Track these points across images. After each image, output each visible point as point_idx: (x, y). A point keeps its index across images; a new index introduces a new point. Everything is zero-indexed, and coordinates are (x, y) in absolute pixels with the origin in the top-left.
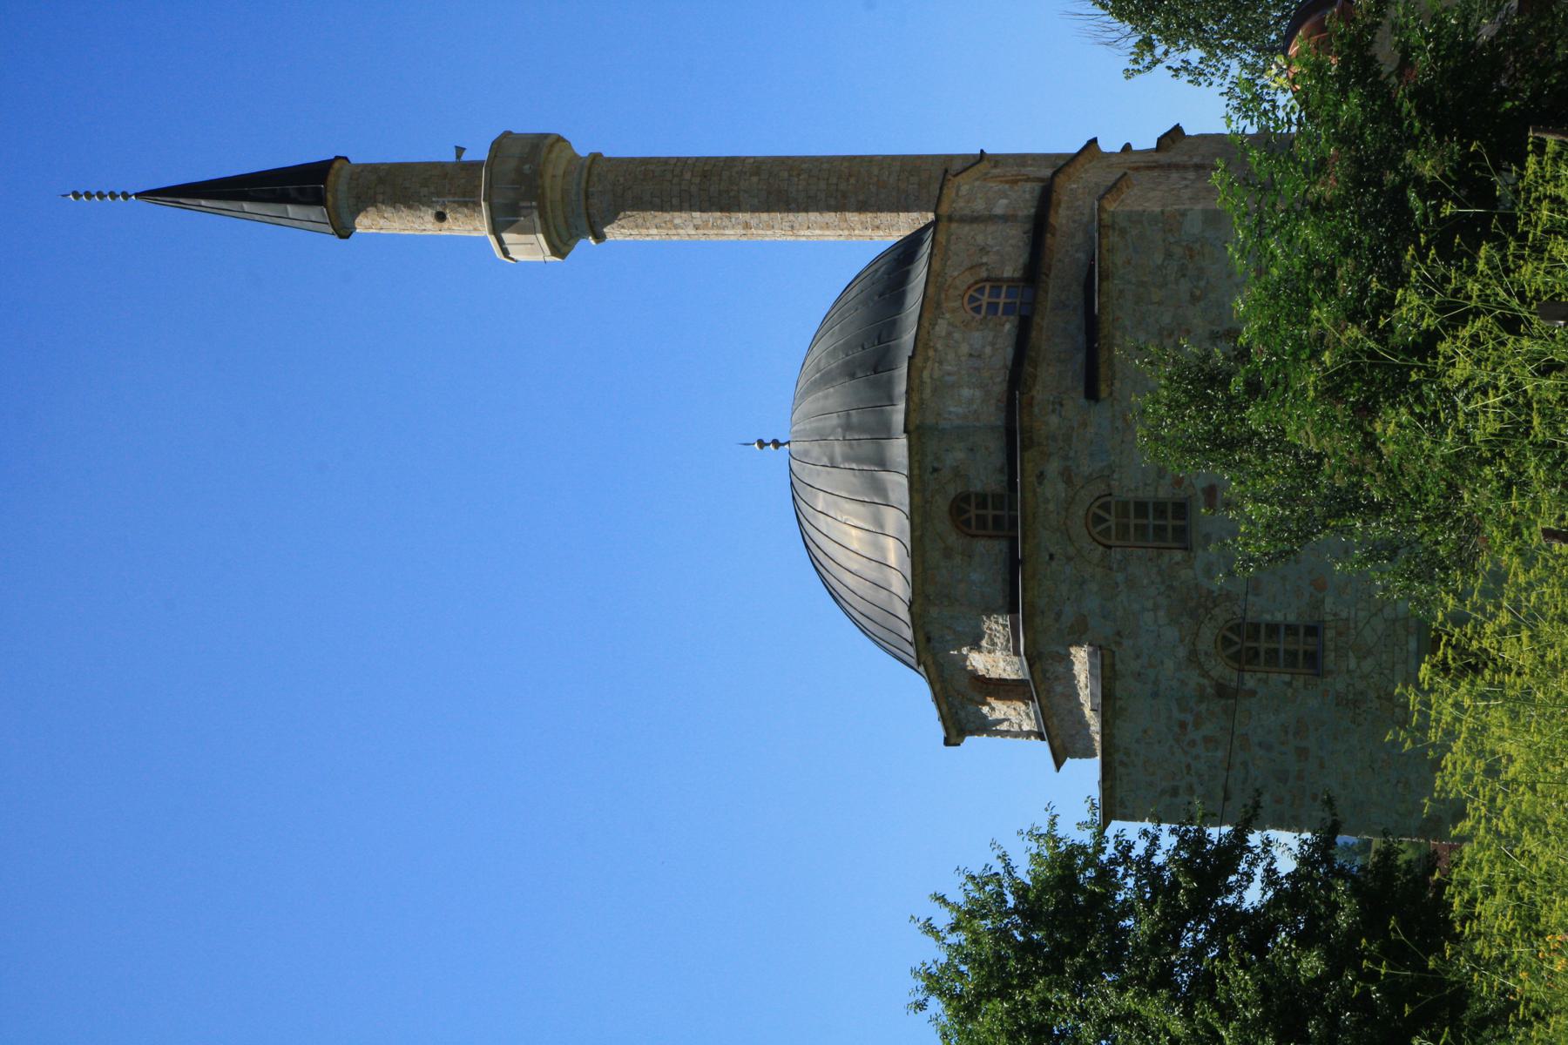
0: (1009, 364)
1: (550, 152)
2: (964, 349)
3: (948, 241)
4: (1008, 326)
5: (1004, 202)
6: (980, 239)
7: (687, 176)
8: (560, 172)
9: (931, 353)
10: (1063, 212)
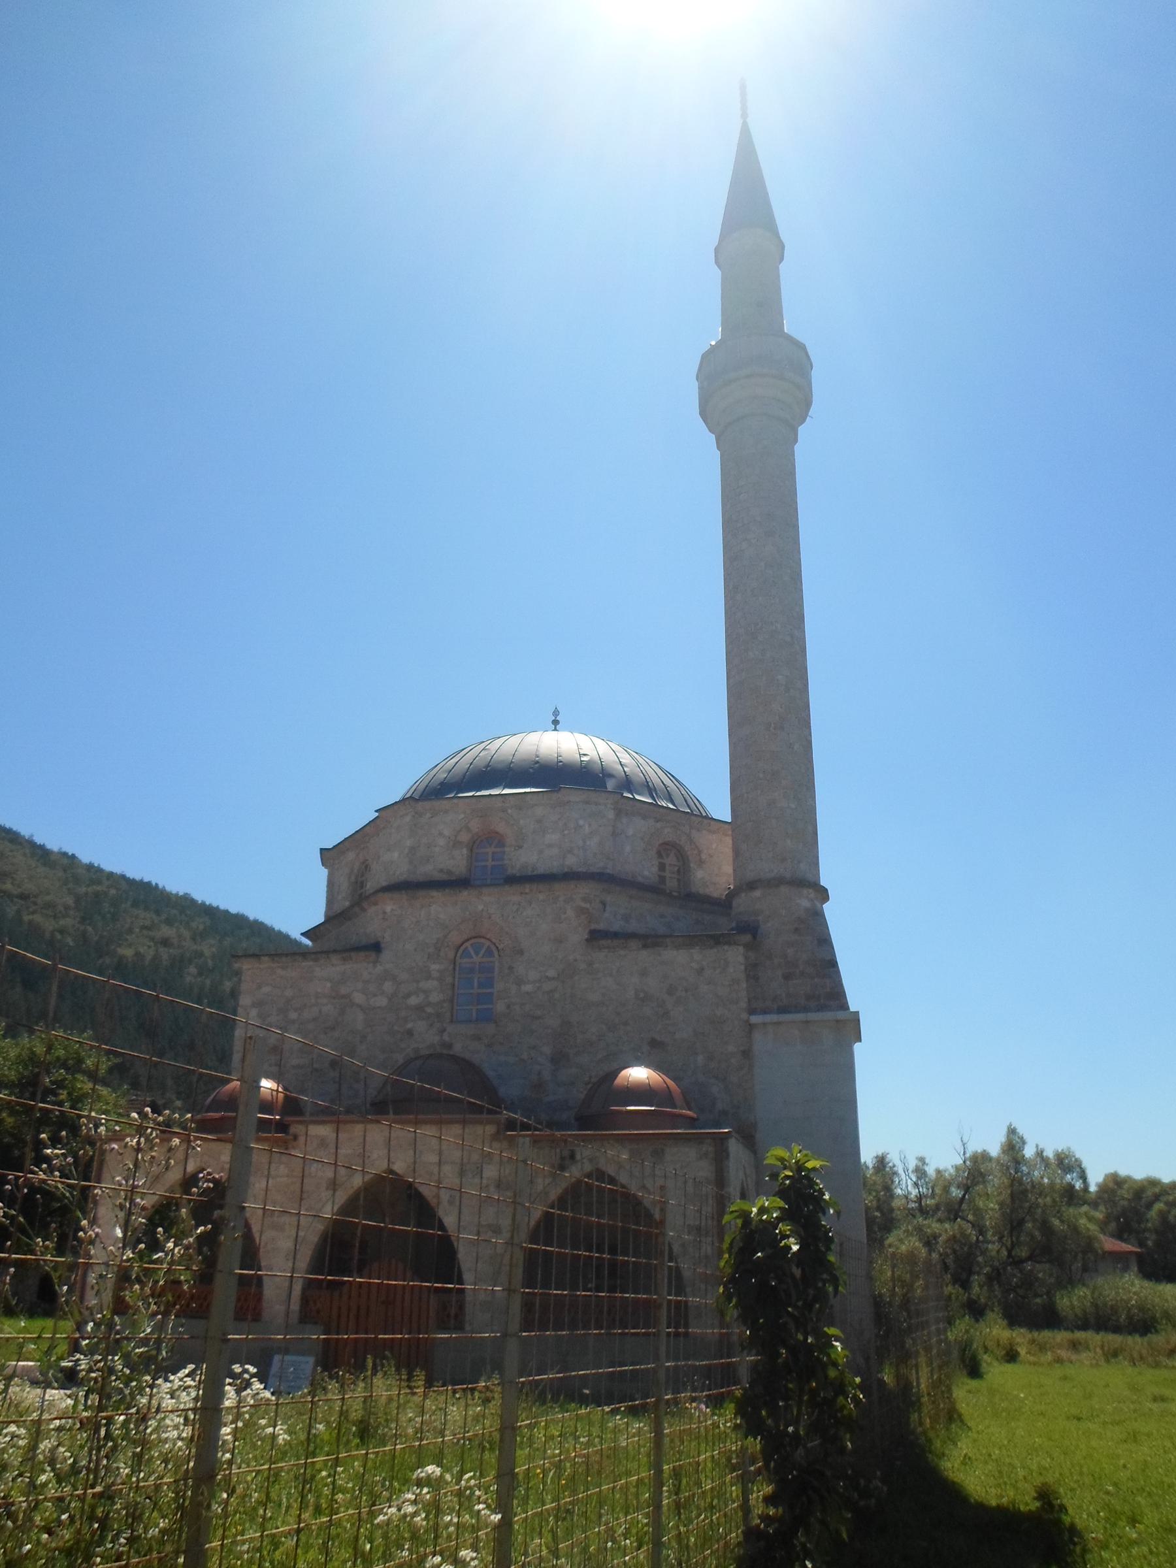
5: (396, 855)
10: (373, 908)
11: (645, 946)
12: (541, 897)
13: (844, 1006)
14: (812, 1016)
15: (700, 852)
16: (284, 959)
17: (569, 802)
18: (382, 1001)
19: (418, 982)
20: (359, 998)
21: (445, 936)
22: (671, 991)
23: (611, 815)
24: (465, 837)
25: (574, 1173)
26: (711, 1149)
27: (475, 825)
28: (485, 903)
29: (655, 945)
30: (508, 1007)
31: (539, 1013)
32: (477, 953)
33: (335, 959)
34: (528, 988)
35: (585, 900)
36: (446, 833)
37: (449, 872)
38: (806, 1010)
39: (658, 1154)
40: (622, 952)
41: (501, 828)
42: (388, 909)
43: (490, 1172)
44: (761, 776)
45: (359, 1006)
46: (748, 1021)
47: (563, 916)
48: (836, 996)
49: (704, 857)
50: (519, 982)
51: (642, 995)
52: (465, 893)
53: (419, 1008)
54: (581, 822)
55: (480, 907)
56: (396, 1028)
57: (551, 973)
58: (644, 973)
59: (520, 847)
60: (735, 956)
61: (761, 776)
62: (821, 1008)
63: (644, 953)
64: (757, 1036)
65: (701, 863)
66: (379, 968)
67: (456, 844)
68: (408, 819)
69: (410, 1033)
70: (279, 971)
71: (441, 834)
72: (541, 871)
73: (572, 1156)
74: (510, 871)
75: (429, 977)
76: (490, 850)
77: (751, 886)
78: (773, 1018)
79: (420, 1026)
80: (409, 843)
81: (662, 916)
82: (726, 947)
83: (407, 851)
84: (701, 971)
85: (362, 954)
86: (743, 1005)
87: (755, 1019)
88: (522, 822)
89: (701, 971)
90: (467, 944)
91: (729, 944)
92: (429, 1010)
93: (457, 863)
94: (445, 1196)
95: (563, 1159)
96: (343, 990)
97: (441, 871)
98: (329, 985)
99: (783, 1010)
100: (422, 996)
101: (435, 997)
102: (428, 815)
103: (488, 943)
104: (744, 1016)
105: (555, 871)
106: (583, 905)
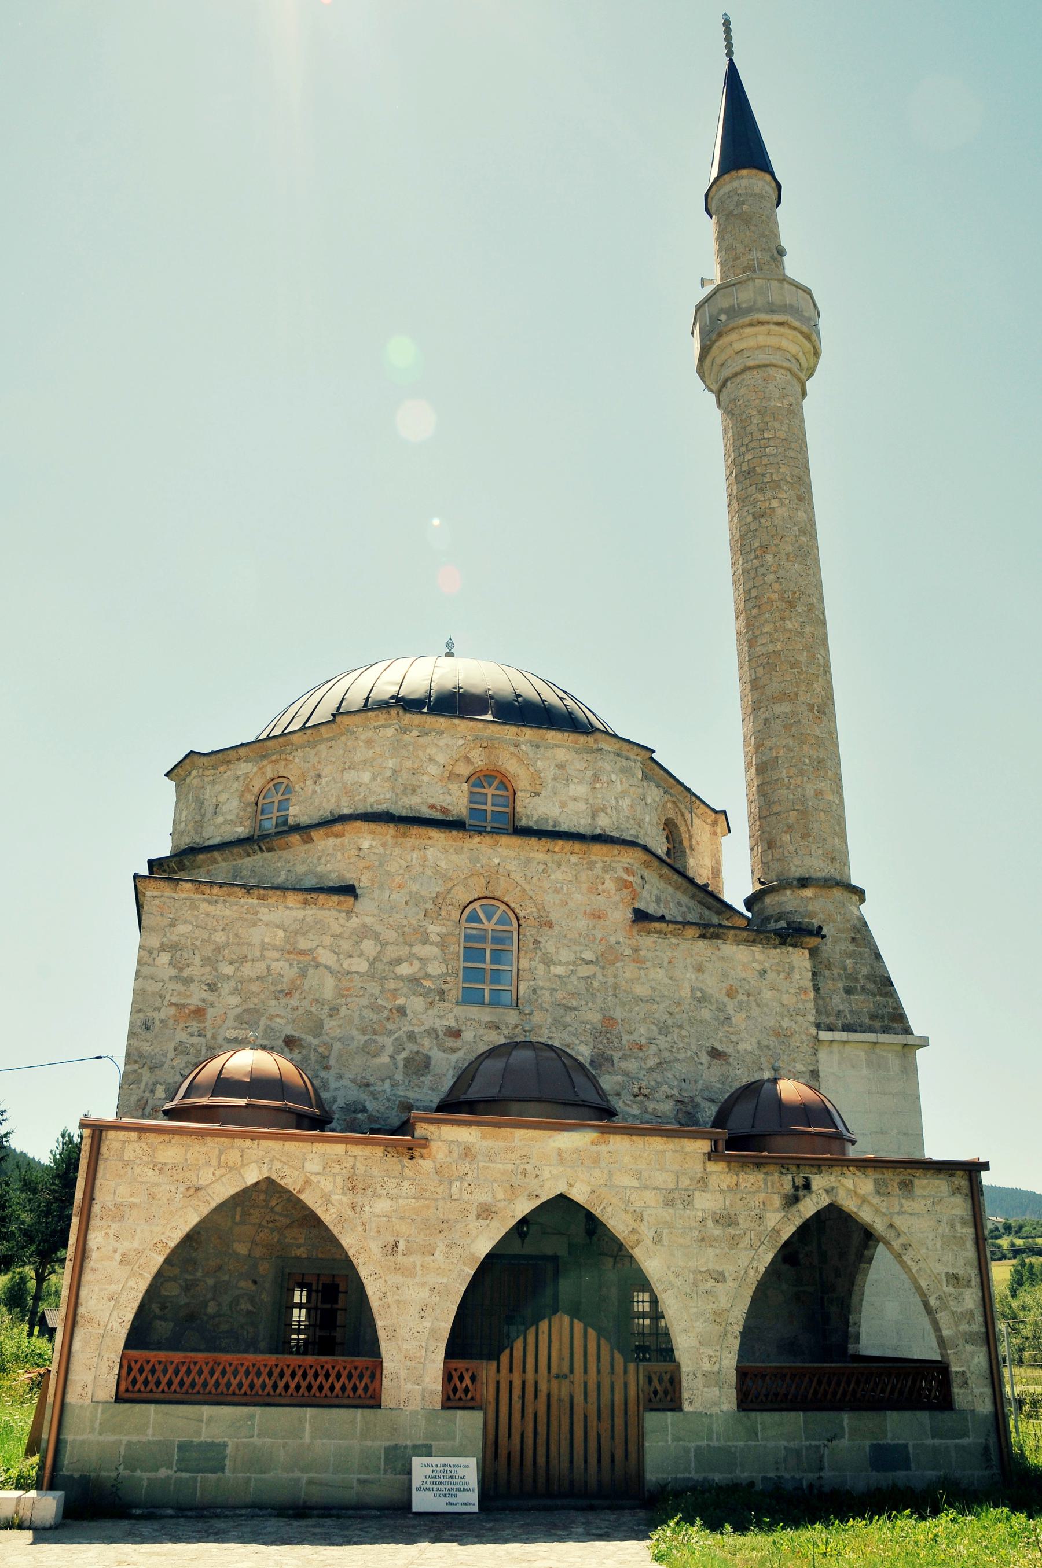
0: (206, 844)
1: (751, 325)
2: (222, 798)
3: (329, 739)
4: (240, 830)
5: (366, 777)
6: (326, 771)
7: (748, 457)
8: (737, 346)
9: (222, 769)
10: (331, 841)
11: (703, 936)
12: (574, 859)
13: (908, 1031)
14: (883, 1038)
15: (691, 837)
16: (216, 890)
17: (601, 749)
18: (363, 966)
19: (411, 946)
20: (325, 957)
21: (449, 891)
22: (731, 993)
23: (640, 776)
24: (465, 770)
25: (809, 1207)
26: (964, 1183)
27: (479, 759)
28: (504, 855)
29: (717, 936)
30: (534, 991)
31: (574, 1003)
32: (489, 919)
33: (292, 899)
34: (559, 970)
35: (627, 870)
36: (441, 759)
37: (444, 810)
38: (871, 1030)
39: (906, 1186)
40: (674, 940)
41: (511, 766)
42: (366, 844)
43: (707, 1202)
44: (807, 761)
45: (326, 967)
46: (816, 1037)
47: (600, 887)
48: (893, 1019)
49: (694, 843)
50: (548, 962)
51: (699, 994)
52: (477, 839)
53: (414, 980)
54: (613, 777)
55: (496, 861)
56: (380, 1002)
57: (588, 955)
58: (699, 969)
59: (537, 794)
60: (799, 959)
61: (807, 761)
62: (885, 1030)
63: (701, 944)
64: (822, 1055)
65: (692, 848)
66: (355, 922)
67: (453, 776)
68: (390, 732)
69: (402, 1011)
70: (204, 906)
71: (431, 760)
72: (564, 828)
73: (807, 1186)
74: (524, 822)
75: (425, 941)
76: (490, 791)
77: (784, 884)
78: (844, 1036)
79: (416, 1004)
80: (391, 763)
81: (679, 904)
82: (791, 949)
83: (388, 773)
84: (763, 973)
85: (335, 898)
86: (812, 1019)
87: (824, 1035)
88: (539, 763)
89: (763, 973)
90: (476, 905)
91: (795, 946)
92: (427, 983)
93: (456, 800)
94: (647, 1232)
95: (796, 1188)
96: (303, 944)
97: (433, 807)
98: (281, 933)
99: (848, 1028)
100: (417, 964)
101: (435, 969)
102: (415, 733)
103: (503, 907)
104: (813, 1030)
105: (582, 831)
106: (625, 877)
